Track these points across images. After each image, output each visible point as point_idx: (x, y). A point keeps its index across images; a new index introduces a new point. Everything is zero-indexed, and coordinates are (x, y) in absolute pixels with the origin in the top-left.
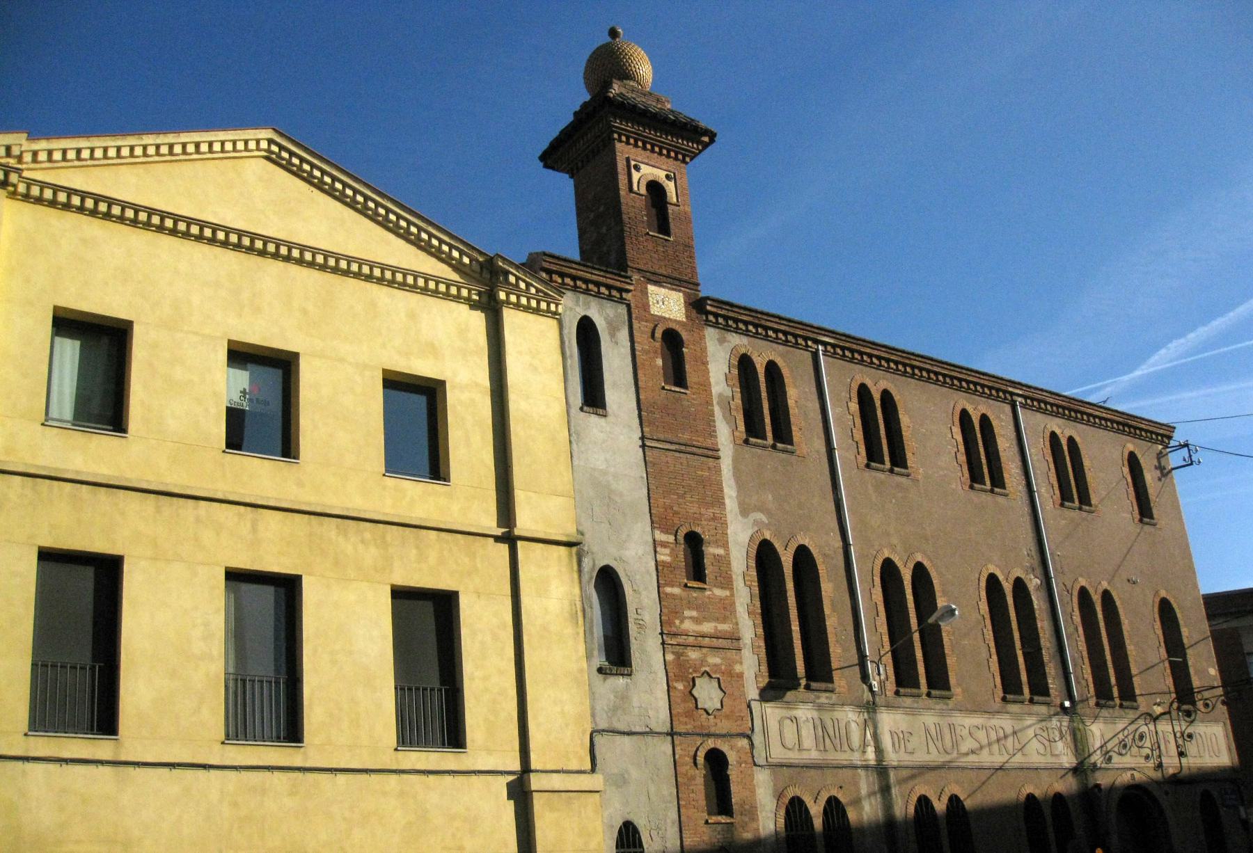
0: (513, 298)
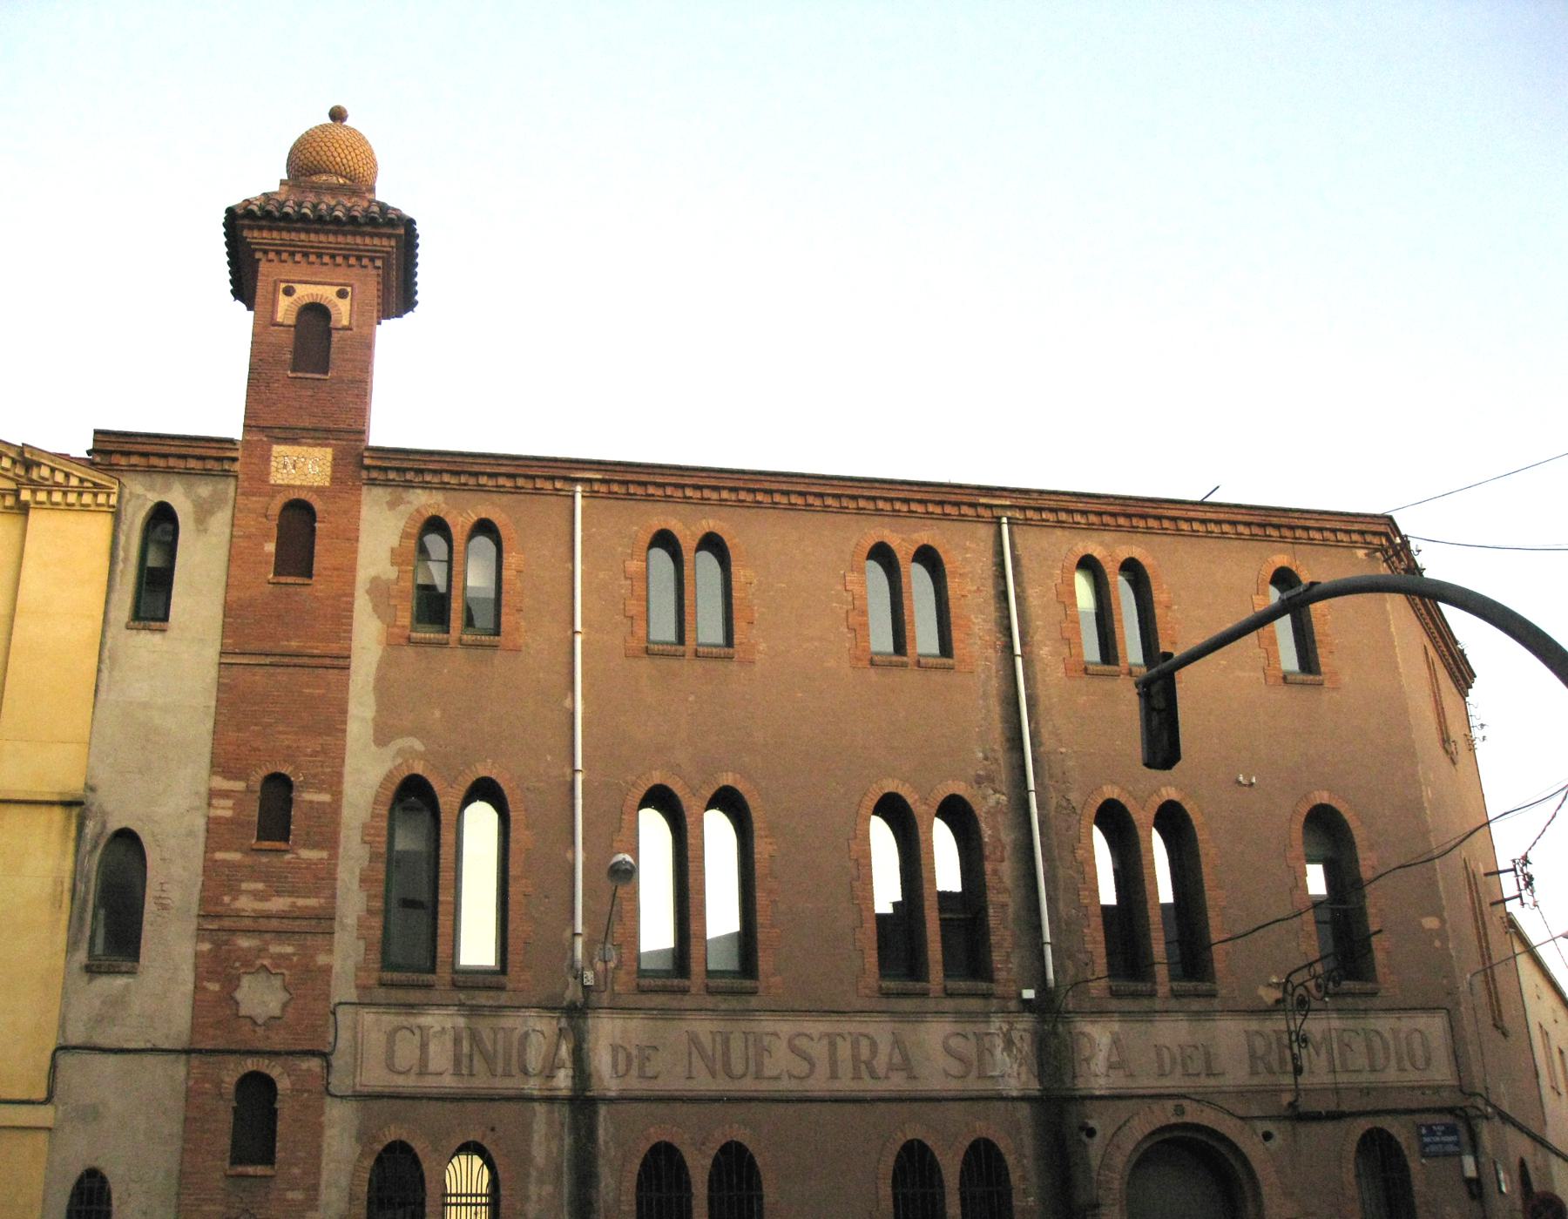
0: (42, 496)
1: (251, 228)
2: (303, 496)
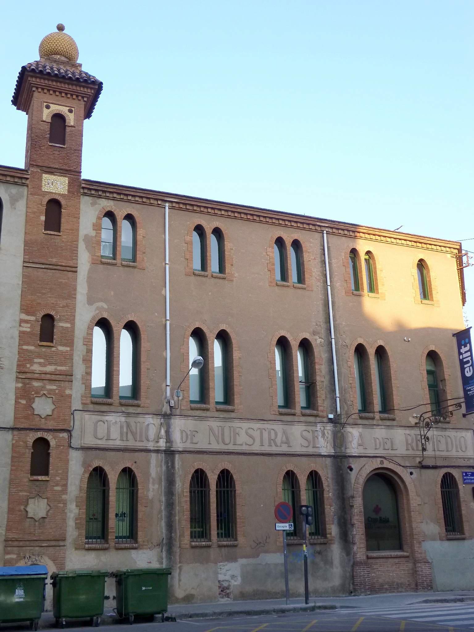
1: (32, 77)
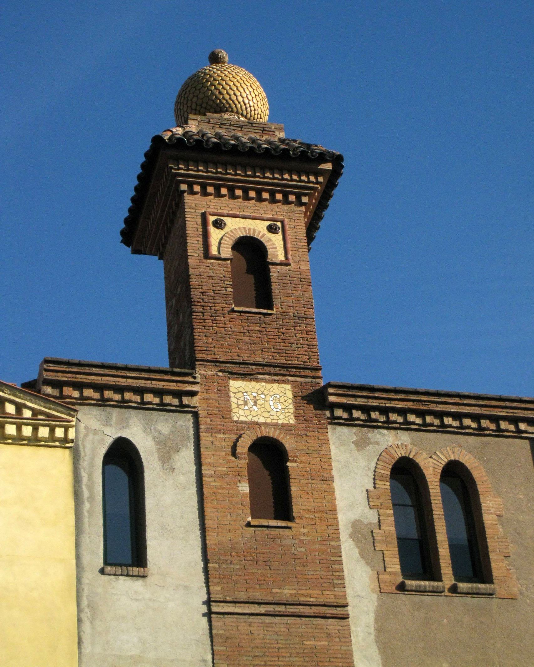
2: (271, 433)
